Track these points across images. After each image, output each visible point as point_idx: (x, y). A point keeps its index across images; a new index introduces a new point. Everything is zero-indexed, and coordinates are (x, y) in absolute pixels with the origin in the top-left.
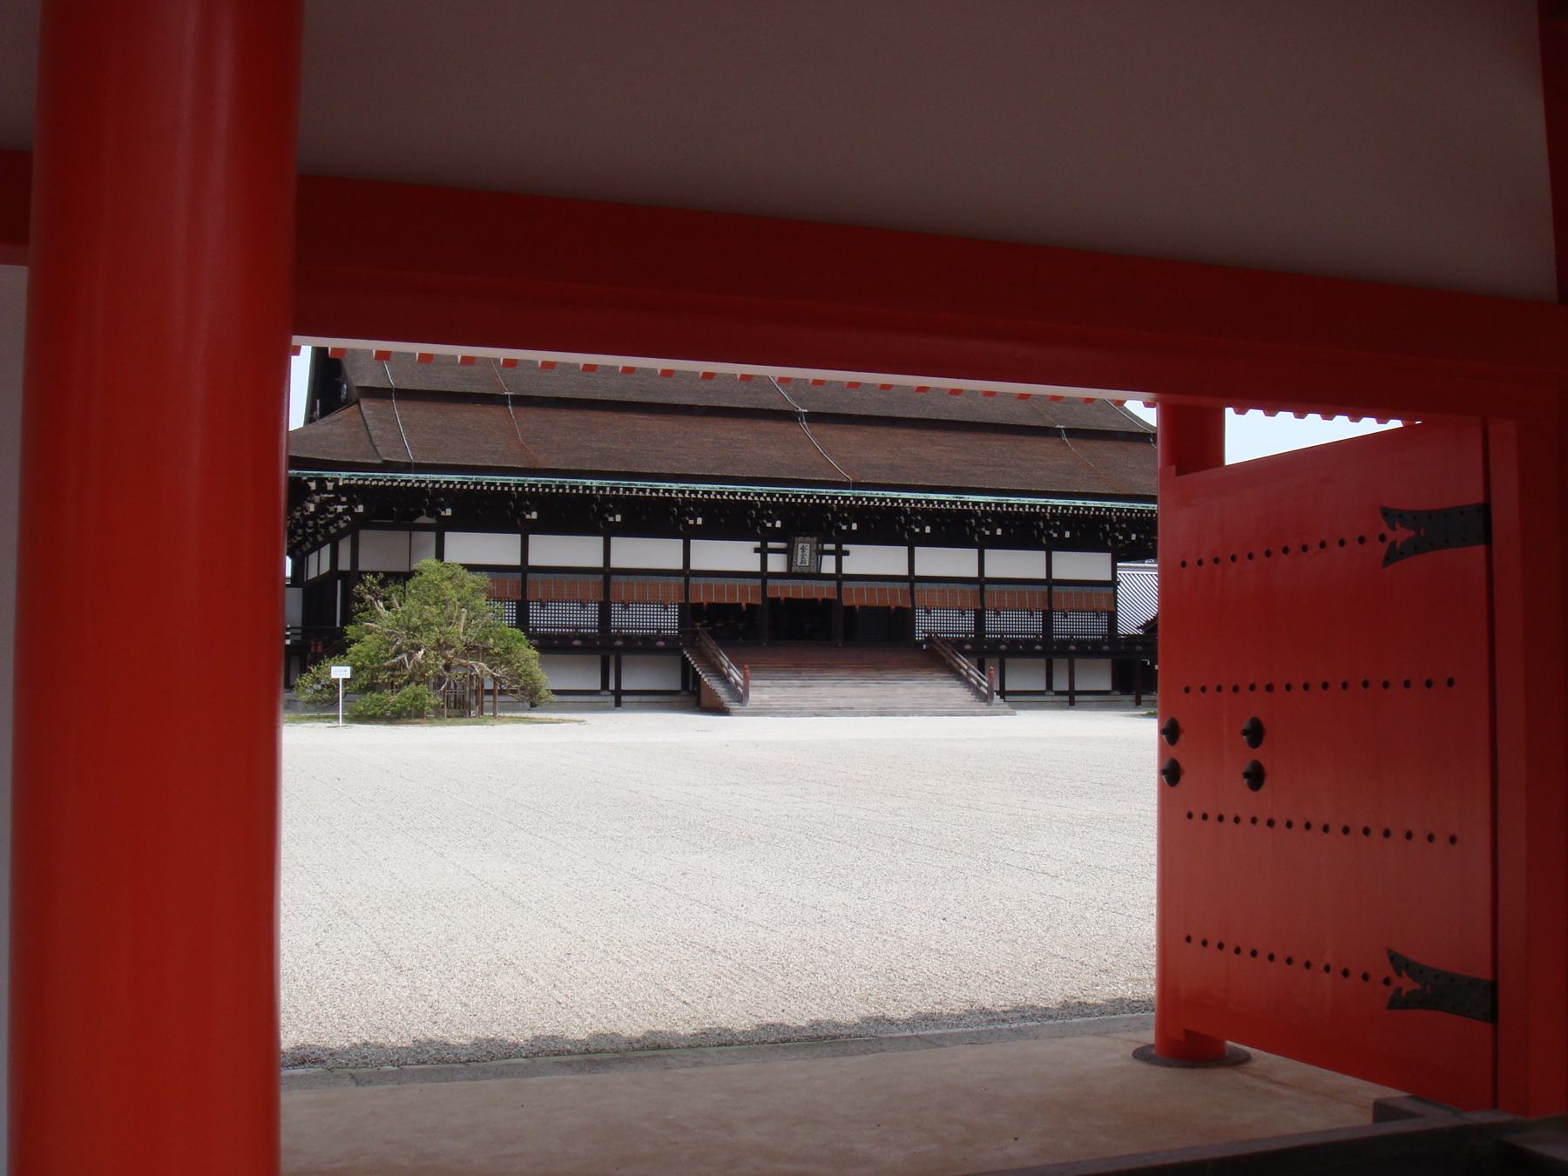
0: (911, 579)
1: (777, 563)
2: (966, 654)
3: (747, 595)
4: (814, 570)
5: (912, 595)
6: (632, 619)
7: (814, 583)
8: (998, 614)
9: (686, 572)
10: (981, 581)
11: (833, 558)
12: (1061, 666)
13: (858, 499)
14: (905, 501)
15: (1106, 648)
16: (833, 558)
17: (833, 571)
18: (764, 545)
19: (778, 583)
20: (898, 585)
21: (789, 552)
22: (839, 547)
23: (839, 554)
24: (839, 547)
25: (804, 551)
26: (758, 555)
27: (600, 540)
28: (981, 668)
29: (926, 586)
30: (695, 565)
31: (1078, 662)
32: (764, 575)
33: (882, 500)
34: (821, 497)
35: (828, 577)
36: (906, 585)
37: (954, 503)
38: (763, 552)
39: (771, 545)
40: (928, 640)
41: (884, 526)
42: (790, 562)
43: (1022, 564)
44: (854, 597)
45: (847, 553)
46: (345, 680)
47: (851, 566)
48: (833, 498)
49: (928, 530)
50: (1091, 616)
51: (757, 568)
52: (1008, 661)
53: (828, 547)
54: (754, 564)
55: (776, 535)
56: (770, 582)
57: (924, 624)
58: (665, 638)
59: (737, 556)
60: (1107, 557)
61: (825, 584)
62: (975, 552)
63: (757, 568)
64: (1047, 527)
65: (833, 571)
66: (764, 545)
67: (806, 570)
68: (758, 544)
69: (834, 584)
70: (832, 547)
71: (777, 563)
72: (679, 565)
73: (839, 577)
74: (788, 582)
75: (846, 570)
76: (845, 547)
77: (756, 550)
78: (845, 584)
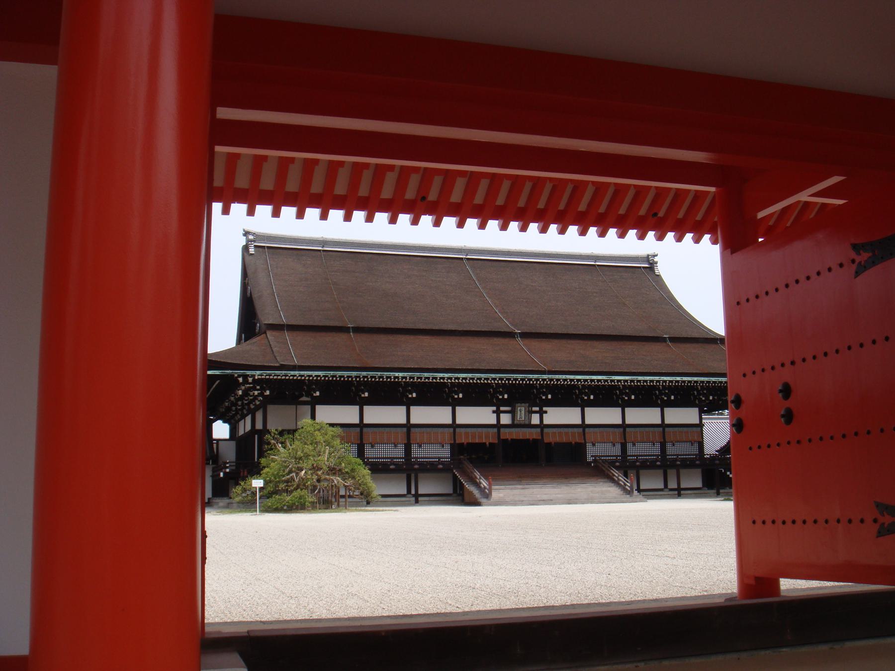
0: (583, 426)
1: (506, 419)
2: (617, 468)
3: (489, 438)
4: (527, 422)
5: (584, 434)
6: (423, 452)
7: (527, 430)
8: (634, 445)
9: (454, 426)
10: (624, 426)
11: (538, 415)
12: (672, 474)
13: (551, 380)
14: (578, 380)
16: (538, 415)
18: (498, 409)
19: (507, 430)
20: (576, 430)
21: (513, 412)
22: (541, 409)
23: (542, 413)
24: (541, 409)
25: (521, 412)
26: (495, 415)
27: (404, 408)
28: (626, 475)
29: (592, 430)
30: (459, 421)
31: (682, 471)
32: (498, 426)
33: (565, 380)
34: (530, 380)
35: (535, 426)
36: (581, 430)
37: (606, 381)
38: (498, 413)
39: (502, 409)
40: (595, 461)
41: (566, 396)
42: (513, 418)
43: (647, 416)
44: (551, 437)
45: (546, 412)
46: (261, 489)
47: (549, 419)
48: (537, 380)
49: (592, 397)
50: (689, 444)
52: (641, 472)
53: (535, 409)
54: (491, 419)
55: (505, 403)
56: (502, 430)
57: (591, 452)
58: (442, 463)
59: (482, 415)
60: (696, 410)
61: (533, 430)
62: (620, 409)
63: (494, 422)
64: (661, 394)
66: (498, 409)
67: (522, 423)
68: (494, 408)
69: (539, 430)
70: (537, 409)
71: (506, 419)
72: (450, 422)
73: (542, 426)
74: (513, 430)
75: (545, 422)
76: (544, 409)
77: (494, 412)
78: (546, 430)
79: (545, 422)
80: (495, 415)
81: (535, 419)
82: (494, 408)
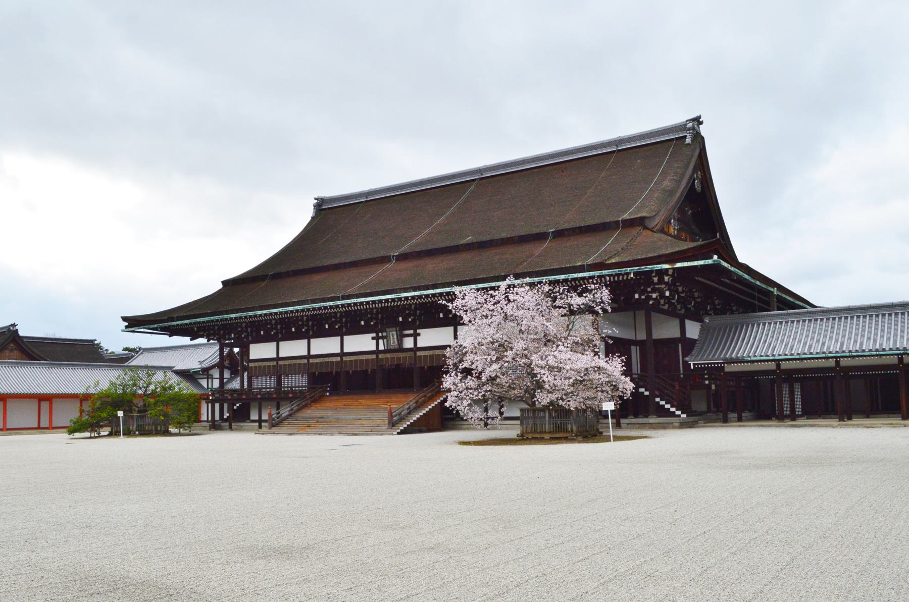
7: (401, 355)
11: (412, 339)
15: (274, 396)
16: (412, 339)
22: (415, 331)
23: (416, 336)
24: (415, 331)
25: (393, 336)
26: (375, 341)
32: (377, 352)
38: (377, 339)
45: (419, 335)
46: (612, 411)
51: (374, 349)
54: (373, 347)
59: (361, 343)
63: (374, 349)
66: (377, 335)
68: (374, 335)
70: (411, 332)
73: (416, 349)
74: (388, 356)
75: (419, 345)
76: (419, 331)
77: (373, 338)
79: (419, 345)
80: (375, 341)
81: (408, 343)
82: (374, 335)
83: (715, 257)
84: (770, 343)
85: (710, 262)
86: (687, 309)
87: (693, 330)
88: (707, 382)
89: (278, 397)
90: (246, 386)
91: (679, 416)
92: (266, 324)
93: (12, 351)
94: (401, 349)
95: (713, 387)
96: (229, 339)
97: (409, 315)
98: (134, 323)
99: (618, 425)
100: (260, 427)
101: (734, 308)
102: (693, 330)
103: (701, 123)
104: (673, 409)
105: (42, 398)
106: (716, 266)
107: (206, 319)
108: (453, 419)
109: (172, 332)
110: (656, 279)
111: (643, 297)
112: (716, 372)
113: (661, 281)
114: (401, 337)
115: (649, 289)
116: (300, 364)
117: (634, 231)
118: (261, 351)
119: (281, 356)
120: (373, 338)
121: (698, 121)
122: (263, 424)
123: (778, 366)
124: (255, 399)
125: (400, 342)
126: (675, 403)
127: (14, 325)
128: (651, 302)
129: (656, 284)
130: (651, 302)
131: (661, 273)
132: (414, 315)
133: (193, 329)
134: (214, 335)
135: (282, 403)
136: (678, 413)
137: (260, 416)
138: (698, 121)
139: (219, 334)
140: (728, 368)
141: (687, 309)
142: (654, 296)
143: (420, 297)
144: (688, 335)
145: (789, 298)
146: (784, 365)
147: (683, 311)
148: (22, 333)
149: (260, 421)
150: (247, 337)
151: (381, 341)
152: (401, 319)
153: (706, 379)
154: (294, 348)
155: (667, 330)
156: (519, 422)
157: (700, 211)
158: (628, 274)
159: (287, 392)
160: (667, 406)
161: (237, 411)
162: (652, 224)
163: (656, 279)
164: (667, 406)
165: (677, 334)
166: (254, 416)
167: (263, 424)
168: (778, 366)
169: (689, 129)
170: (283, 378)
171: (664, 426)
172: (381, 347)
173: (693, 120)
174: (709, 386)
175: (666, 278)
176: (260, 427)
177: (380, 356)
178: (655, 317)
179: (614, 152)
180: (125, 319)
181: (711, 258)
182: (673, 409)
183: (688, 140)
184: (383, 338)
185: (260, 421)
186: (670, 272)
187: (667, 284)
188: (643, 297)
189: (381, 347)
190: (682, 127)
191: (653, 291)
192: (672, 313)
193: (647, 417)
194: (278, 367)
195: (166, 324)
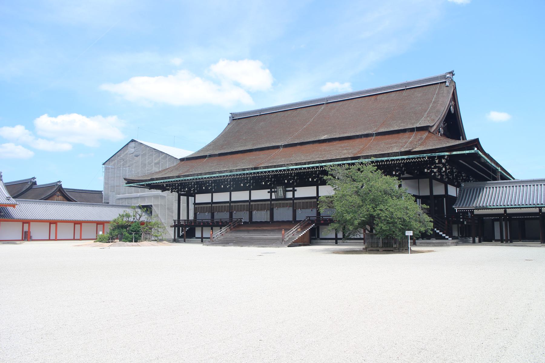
17: (292, 197)
22: (294, 189)
23: (294, 191)
24: (294, 189)
25: (280, 190)
32: (271, 200)
38: (271, 192)
39: (273, 190)
45: (296, 190)
51: (269, 198)
54: (268, 197)
63: (269, 198)
65: (292, 197)
66: (271, 190)
68: (269, 190)
70: (291, 189)
73: (294, 199)
75: (296, 196)
76: (295, 188)
77: (268, 192)
79: (296, 196)
81: (289, 195)
83: (476, 149)
84: (492, 198)
85: (472, 151)
86: (449, 179)
87: (452, 191)
88: (461, 220)
89: (213, 224)
90: (191, 217)
91: (447, 239)
92: (206, 183)
93: (58, 196)
94: (285, 199)
95: (465, 223)
96: (184, 191)
97: (291, 179)
98: (129, 182)
99: (414, 244)
100: (202, 241)
101: (471, 179)
102: (452, 191)
103: (453, 75)
104: (444, 235)
105: (76, 223)
106: (476, 155)
107: (174, 180)
108: (315, 239)
109: (151, 187)
110: (437, 161)
111: (429, 171)
112: (464, 213)
113: (440, 162)
114: (285, 191)
115: (433, 167)
116: (225, 206)
117: (425, 134)
118: (203, 198)
119: (214, 201)
120: (268, 192)
121: (452, 73)
122: (204, 240)
123: (505, 211)
124: (199, 226)
125: (285, 195)
126: (445, 232)
127: (60, 182)
128: (433, 174)
129: (437, 164)
130: (433, 174)
131: (440, 158)
132: (294, 179)
133: (163, 185)
134: (175, 189)
135: (214, 228)
136: (447, 237)
137: (336, 235)
138: (452, 73)
139: (178, 188)
140: (476, 212)
141: (449, 179)
142: (435, 170)
143: (300, 169)
144: (449, 194)
145: (505, 174)
146: (509, 211)
147: (446, 180)
148: (63, 187)
149: (202, 238)
150: (194, 190)
151: (273, 194)
152: (286, 181)
153: (461, 218)
154: (221, 197)
155: (439, 190)
156: (363, 241)
157: (452, 124)
158: (425, 157)
159: (217, 222)
160: (441, 233)
161: (186, 231)
162: (432, 130)
163: (437, 161)
164: (441, 233)
165: (443, 193)
166: (198, 234)
167: (338, 241)
168: (505, 211)
169: (448, 78)
170: (215, 214)
171: (441, 245)
172: (273, 197)
173: (450, 73)
174: (463, 222)
175: (443, 161)
176: (202, 241)
177: (272, 202)
178: (434, 182)
179: (404, 89)
180: (125, 179)
181: (474, 149)
182: (444, 235)
183: (447, 84)
184: (274, 192)
185: (202, 238)
186: (446, 157)
187: (443, 164)
188: (429, 171)
189: (273, 197)
190: (444, 77)
191: (435, 168)
192: (441, 181)
193: (430, 239)
194: (212, 207)
195: (150, 182)
